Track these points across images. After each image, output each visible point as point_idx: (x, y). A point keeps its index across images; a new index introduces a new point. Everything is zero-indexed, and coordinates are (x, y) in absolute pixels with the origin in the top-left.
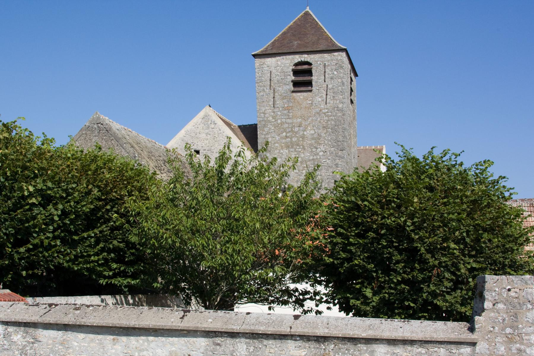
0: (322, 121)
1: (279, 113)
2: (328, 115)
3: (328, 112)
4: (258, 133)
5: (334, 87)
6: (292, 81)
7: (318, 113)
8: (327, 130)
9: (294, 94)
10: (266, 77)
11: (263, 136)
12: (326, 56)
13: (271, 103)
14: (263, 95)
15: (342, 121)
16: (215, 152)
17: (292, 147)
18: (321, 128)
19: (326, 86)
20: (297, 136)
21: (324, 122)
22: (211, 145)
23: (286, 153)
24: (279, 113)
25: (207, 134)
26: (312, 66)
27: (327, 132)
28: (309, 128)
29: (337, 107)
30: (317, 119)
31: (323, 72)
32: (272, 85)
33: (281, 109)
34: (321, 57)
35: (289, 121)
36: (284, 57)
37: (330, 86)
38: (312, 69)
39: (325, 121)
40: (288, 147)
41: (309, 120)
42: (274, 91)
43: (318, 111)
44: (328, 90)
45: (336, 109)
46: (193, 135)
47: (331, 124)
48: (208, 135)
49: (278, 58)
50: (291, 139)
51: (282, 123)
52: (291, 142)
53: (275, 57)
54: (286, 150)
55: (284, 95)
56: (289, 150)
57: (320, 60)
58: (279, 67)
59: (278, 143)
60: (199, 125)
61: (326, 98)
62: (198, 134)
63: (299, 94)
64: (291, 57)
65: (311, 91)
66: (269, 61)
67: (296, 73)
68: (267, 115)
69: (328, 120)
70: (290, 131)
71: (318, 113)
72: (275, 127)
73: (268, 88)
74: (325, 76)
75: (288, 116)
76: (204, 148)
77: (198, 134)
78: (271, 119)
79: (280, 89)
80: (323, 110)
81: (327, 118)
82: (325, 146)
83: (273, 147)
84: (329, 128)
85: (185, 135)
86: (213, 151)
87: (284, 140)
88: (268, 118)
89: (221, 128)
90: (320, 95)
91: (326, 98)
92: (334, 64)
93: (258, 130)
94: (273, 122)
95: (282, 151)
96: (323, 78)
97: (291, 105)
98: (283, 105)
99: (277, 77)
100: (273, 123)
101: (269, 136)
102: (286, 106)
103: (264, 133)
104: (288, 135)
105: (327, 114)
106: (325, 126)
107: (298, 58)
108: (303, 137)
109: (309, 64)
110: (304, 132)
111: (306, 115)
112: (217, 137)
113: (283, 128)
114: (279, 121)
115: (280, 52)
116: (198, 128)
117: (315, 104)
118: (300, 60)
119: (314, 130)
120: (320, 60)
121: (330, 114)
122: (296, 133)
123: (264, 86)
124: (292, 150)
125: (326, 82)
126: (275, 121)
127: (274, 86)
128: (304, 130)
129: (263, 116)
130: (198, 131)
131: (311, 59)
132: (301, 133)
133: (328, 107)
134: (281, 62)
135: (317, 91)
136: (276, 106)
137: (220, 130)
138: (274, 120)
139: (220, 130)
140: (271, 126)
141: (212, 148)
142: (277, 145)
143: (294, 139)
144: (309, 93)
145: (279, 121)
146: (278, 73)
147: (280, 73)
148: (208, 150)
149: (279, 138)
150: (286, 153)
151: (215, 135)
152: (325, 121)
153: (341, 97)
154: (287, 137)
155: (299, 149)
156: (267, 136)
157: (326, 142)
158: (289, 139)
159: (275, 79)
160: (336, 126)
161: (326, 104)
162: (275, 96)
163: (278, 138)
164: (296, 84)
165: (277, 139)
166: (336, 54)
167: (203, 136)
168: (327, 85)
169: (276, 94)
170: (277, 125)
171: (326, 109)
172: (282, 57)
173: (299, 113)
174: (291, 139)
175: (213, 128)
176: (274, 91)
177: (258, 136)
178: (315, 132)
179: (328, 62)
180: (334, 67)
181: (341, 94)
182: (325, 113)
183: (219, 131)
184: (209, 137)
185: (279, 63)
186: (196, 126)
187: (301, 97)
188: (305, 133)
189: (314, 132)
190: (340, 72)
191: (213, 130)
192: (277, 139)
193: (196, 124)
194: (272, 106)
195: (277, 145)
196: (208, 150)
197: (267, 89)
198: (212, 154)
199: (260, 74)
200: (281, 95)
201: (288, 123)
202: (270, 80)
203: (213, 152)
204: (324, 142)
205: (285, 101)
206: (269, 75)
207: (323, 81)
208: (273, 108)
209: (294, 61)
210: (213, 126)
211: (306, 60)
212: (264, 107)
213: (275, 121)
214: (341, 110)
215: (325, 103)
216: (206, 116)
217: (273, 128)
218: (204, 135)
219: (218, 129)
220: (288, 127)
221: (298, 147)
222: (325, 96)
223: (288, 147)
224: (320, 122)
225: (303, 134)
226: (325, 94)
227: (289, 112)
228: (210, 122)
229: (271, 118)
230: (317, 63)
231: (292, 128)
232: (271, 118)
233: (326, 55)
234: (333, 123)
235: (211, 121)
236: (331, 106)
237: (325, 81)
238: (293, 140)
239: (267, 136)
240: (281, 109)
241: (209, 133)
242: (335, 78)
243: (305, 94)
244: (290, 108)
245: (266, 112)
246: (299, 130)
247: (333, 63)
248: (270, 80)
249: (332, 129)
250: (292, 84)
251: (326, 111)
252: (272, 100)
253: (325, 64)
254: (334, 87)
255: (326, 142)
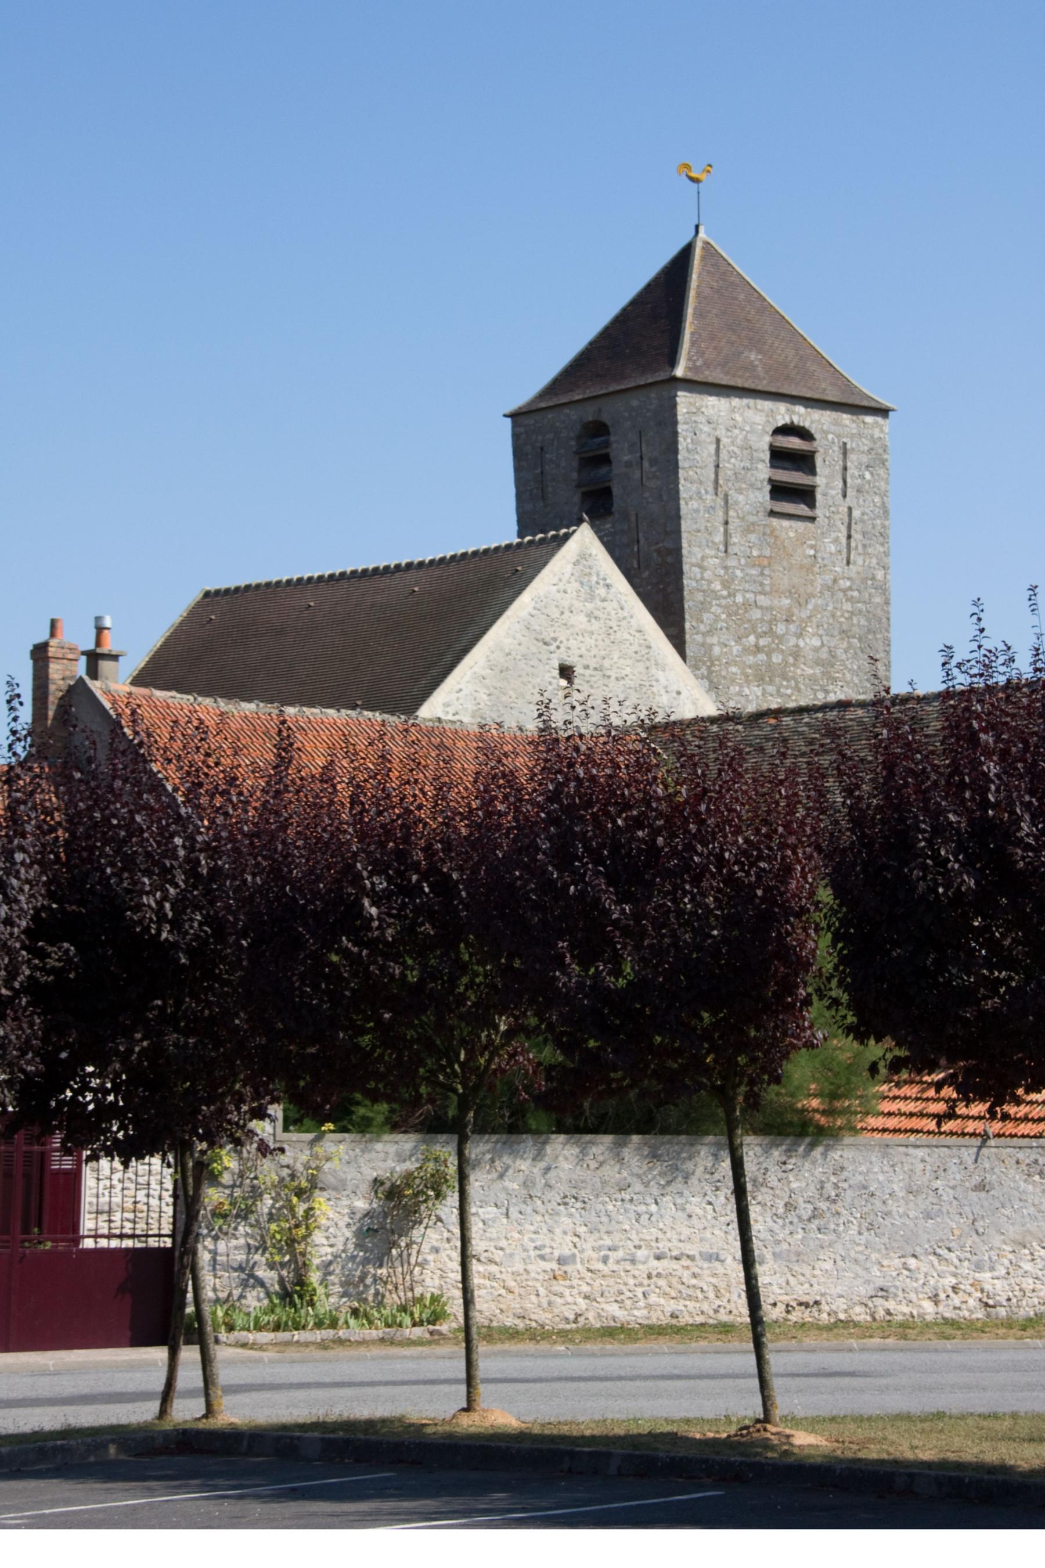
0: (839, 614)
1: (738, 573)
2: (852, 597)
3: (850, 589)
4: (687, 625)
5: (866, 517)
6: (770, 480)
7: (829, 588)
8: (848, 642)
9: (775, 522)
10: (705, 455)
11: (699, 638)
12: (847, 422)
13: (719, 538)
14: (697, 511)
15: (884, 620)
16: (613, 678)
17: (771, 682)
18: (836, 633)
19: (846, 510)
20: (782, 651)
21: (842, 616)
22: (603, 653)
23: (757, 697)
24: (738, 573)
25: (590, 615)
26: (815, 444)
27: (850, 646)
28: (810, 630)
29: (870, 576)
30: (827, 605)
31: (838, 468)
32: (721, 482)
33: (743, 561)
34: (836, 423)
35: (763, 601)
36: (751, 402)
37: (856, 513)
38: (814, 452)
39: (846, 615)
40: (760, 680)
41: (810, 607)
42: (726, 502)
43: (830, 583)
44: (853, 525)
45: (870, 582)
46: (555, 613)
47: (859, 625)
48: (593, 620)
49: (736, 402)
50: (769, 655)
51: (747, 605)
52: (769, 666)
53: (728, 396)
54: (756, 689)
55: (752, 519)
56: (764, 689)
57: (833, 428)
58: (737, 431)
59: (736, 663)
60: (569, 582)
61: (849, 545)
62: (567, 613)
63: (786, 523)
64: (767, 405)
65: (813, 519)
66: (713, 406)
67: (779, 457)
68: (707, 574)
69: (852, 613)
70: (766, 633)
71: (829, 588)
72: (729, 615)
73: (711, 489)
74: (845, 482)
75: (762, 584)
76: (585, 663)
77: (567, 613)
78: (719, 587)
79: (741, 498)
80: (841, 582)
81: (847, 606)
82: (845, 689)
83: (724, 673)
84: (854, 637)
85: (534, 612)
86: (608, 673)
87: (751, 658)
88: (710, 582)
89: (623, 602)
90: (834, 535)
91: (849, 545)
92: (866, 448)
93: (687, 616)
94: (725, 598)
95: (747, 691)
96: (841, 485)
97: (767, 552)
98: (748, 550)
99: (733, 460)
100: (723, 602)
101: (714, 640)
102: (755, 553)
103: (702, 628)
104: (762, 642)
105: (850, 593)
106: (845, 627)
107: (783, 414)
108: (796, 653)
109: (804, 434)
110: (798, 638)
111: (802, 590)
112: (615, 628)
113: (749, 621)
114: (739, 599)
115: (740, 383)
116: (565, 592)
117: (823, 559)
118: (788, 420)
119: (821, 636)
120: (833, 428)
121: (856, 594)
122: (781, 638)
123: (701, 483)
124: (771, 689)
125: (848, 499)
126: (729, 595)
127: (725, 488)
128: (800, 635)
129: (699, 576)
130: (566, 604)
131: (812, 422)
132: (793, 641)
133: (853, 575)
134: (742, 415)
135: (826, 520)
136: (729, 550)
137: (622, 609)
138: (725, 593)
139: (622, 609)
140: (719, 611)
141: (607, 663)
142: (734, 669)
143: (777, 658)
144: (809, 525)
145: (739, 599)
146: (736, 450)
147: (742, 448)
148: (595, 669)
149: (740, 648)
150: (757, 697)
151: (610, 624)
152: (846, 615)
153: (882, 549)
154: (758, 649)
155: (787, 688)
156: (709, 640)
157: (848, 676)
158: (762, 657)
159: (728, 466)
160: (869, 631)
161: (848, 563)
162: (730, 520)
163: (736, 649)
164: (779, 491)
165: (735, 652)
166: (869, 419)
167: (580, 620)
168: (850, 509)
169: (731, 513)
170: (735, 608)
171: (849, 579)
172: (745, 401)
173: (784, 583)
174: (769, 655)
175: (604, 600)
176: (726, 502)
177: (687, 637)
178: (823, 645)
179: (852, 441)
180: (865, 459)
181: (881, 539)
182: (844, 591)
183: (620, 611)
184: (595, 625)
185: (739, 418)
186: (561, 586)
187: (792, 534)
188: (801, 644)
189: (819, 644)
190: (879, 475)
191: (605, 604)
192: (735, 652)
193: (560, 580)
194: (722, 548)
195: (734, 669)
196: (595, 669)
197: (707, 492)
198: (606, 681)
199: (689, 440)
200: (743, 519)
201: (761, 608)
202: (717, 466)
203: (609, 677)
204: (844, 674)
205: (753, 537)
206: (712, 448)
207: (840, 496)
208: (722, 555)
209: (775, 419)
210: (602, 591)
211: (801, 424)
212: (700, 546)
213: (729, 595)
214: (881, 587)
215: (845, 562)
216: (583, 556)
217: (724, 616)
218: (582, 618)
219: (615, 604)
220: (762, 620)
221: (785, 683)
222: (844, 541)
223: (763, 680)
224: (833, 616)
225: (797, 646)
226: (845, 533)
227: (762, 574)
228: (594, 578)
229: (717, 586)
230: (827, 439)
231: (770, 622)
232: (717, 586)
233: (846, 418)
234: (863, 622)
235: (598, 575)
236: (858, 573)
237: (845, 496)
238: (774, 660)
239: (709, 640)
240: (743, 561)
241: (597, 613)
242: (868, 492)
243: (800, 525)
244: (766, 562)
245: (705, 564)
246: (787, 633)
247: (864, 444)
248: (717, 466)
249: (860, 640)
250: (768, 488)
251: (848, 584)
252: (722, 529)
253: (845, 444)
254: (866, 517)
255: (848, 676)
